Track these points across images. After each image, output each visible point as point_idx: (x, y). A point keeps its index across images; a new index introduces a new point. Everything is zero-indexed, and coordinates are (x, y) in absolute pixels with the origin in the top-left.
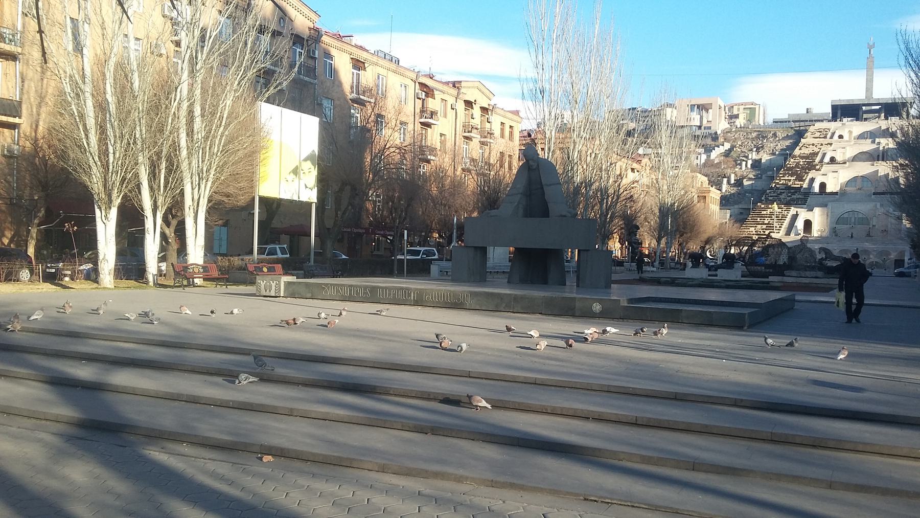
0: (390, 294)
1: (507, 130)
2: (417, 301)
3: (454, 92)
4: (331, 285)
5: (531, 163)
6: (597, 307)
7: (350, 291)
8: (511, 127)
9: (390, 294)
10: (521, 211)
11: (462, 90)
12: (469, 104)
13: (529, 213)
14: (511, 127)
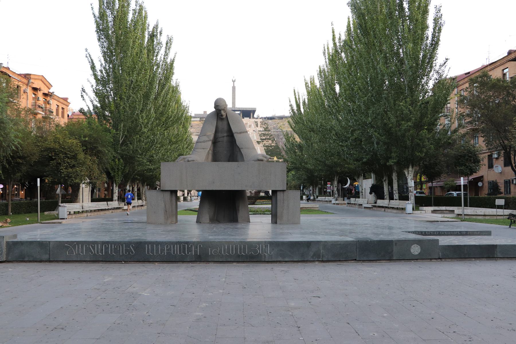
0: (162, 250)
1: (60, 110)
2: (200, 256)
3: (25, 81)
4: (78, 243)
5: (222, 112)
6: (416, 250)
7: (107, 249)
8: (63, 108)
9: (162, 250)
10: (210, 157)
11: (31, 81)
12: (35, 89)
13: (216, 158)
14: (63, 108)
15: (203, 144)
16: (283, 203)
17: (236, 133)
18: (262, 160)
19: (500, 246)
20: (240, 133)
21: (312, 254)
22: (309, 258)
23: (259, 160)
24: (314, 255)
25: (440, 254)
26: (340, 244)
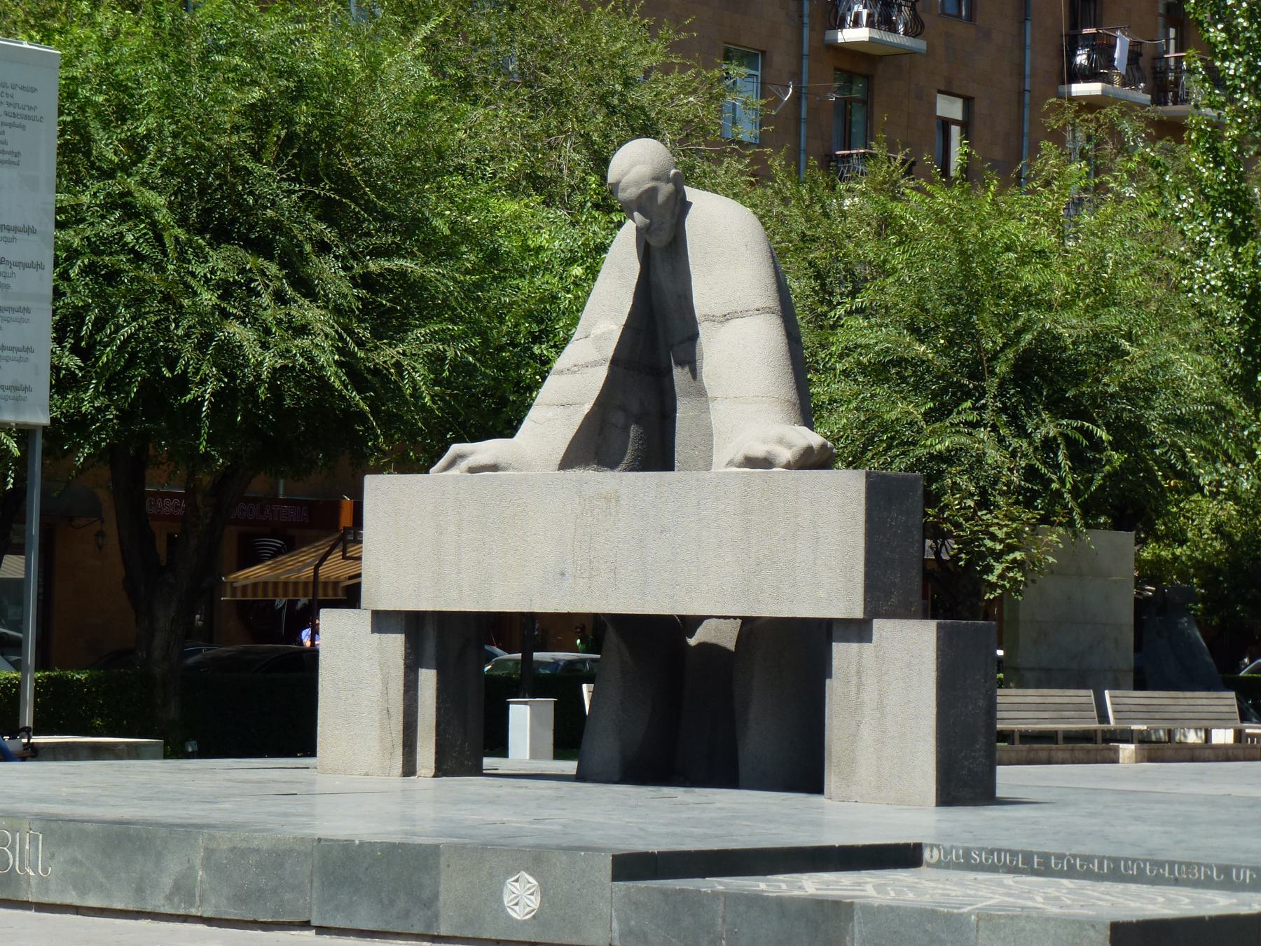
16: (859, 686)
17: (711, 318)
18: (765, 463)
19: (872, 912)
20: (727, 318)
21: (167, 882)
22: (158, 903)
23: (751, 462)
24: (177, 888)
25: (615, 925)
26: (258, 851)
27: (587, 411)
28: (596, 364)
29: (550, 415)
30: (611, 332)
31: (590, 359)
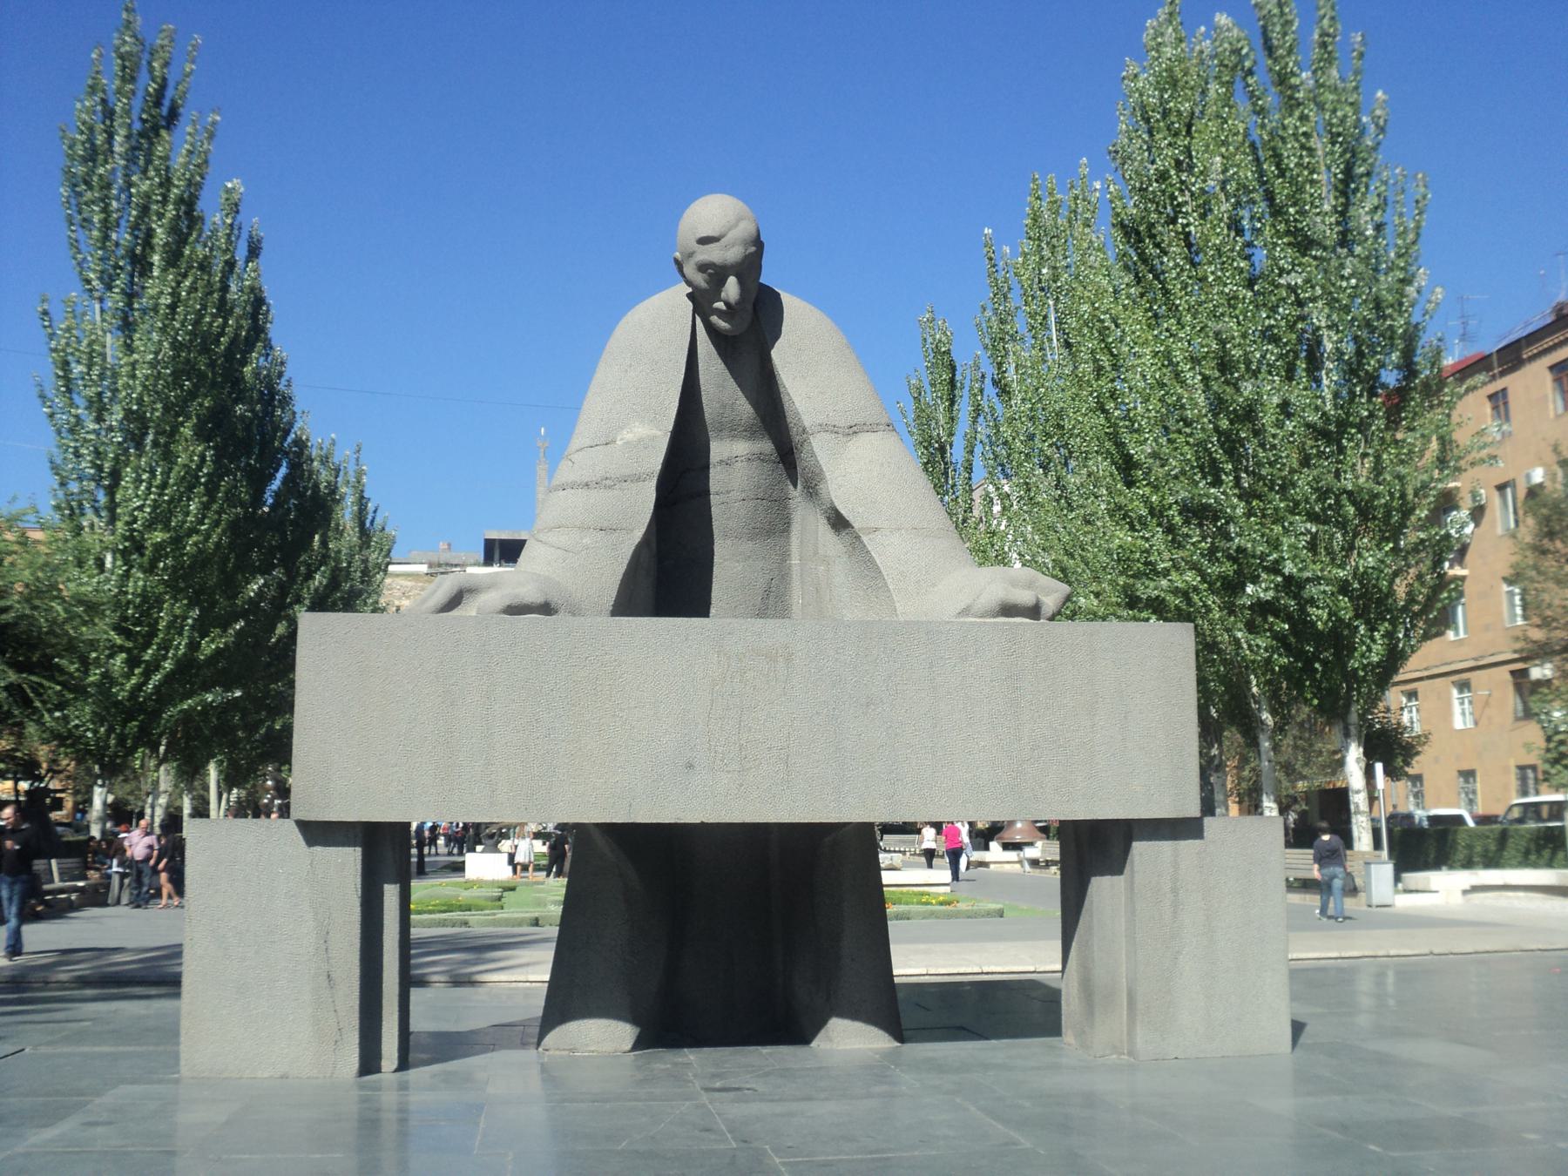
15: (596, 496)
17: (825, 428)
20: (853, 430)
23: (1008, 610)
27: (637, 540)
28: (638, 479)
29: (586, 541)
30: (654, 438)
31: (627, 472)
